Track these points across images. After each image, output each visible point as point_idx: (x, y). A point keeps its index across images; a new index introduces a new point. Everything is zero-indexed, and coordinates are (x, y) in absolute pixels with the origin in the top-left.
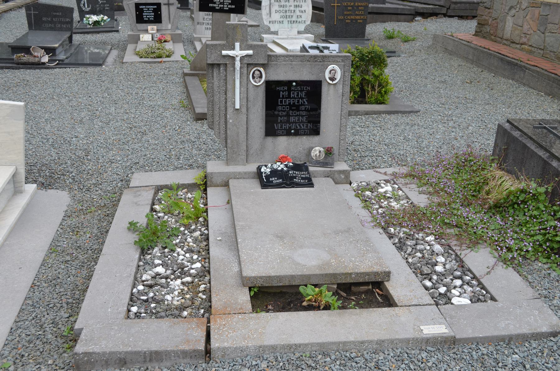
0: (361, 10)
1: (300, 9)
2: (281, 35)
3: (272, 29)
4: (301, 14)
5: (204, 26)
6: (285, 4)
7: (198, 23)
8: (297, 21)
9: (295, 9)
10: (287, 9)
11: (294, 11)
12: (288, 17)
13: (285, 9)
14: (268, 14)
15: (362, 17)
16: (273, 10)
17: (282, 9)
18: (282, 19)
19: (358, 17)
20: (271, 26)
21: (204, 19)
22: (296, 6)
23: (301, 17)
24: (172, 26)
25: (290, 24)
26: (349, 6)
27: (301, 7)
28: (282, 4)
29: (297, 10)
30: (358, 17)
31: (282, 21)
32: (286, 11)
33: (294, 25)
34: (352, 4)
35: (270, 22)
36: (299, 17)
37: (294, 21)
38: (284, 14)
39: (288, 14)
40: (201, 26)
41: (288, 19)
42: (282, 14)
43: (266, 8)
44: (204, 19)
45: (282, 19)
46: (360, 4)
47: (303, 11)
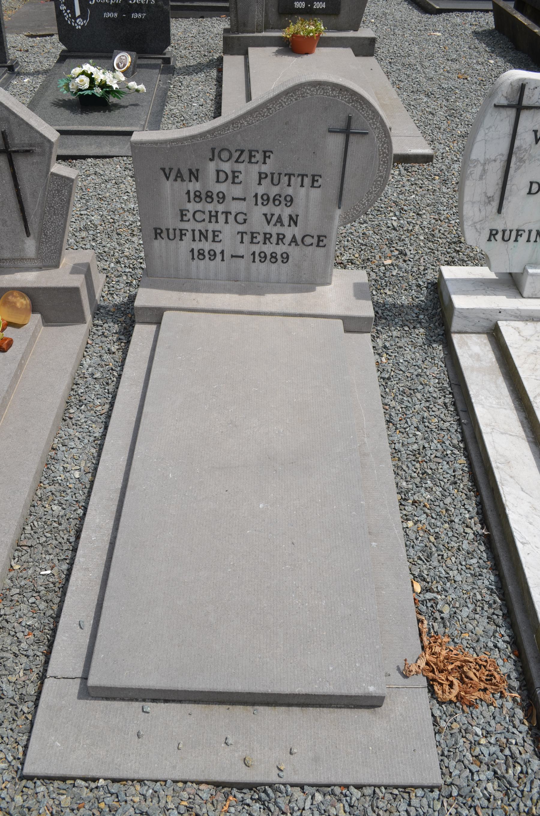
5: (186, 244)
14: (490, 200)
21: (182, 214)
24: (40, 243)
35: (493, 234)
40: (172, 244)
43: (484, 171)
44: (182, 214)
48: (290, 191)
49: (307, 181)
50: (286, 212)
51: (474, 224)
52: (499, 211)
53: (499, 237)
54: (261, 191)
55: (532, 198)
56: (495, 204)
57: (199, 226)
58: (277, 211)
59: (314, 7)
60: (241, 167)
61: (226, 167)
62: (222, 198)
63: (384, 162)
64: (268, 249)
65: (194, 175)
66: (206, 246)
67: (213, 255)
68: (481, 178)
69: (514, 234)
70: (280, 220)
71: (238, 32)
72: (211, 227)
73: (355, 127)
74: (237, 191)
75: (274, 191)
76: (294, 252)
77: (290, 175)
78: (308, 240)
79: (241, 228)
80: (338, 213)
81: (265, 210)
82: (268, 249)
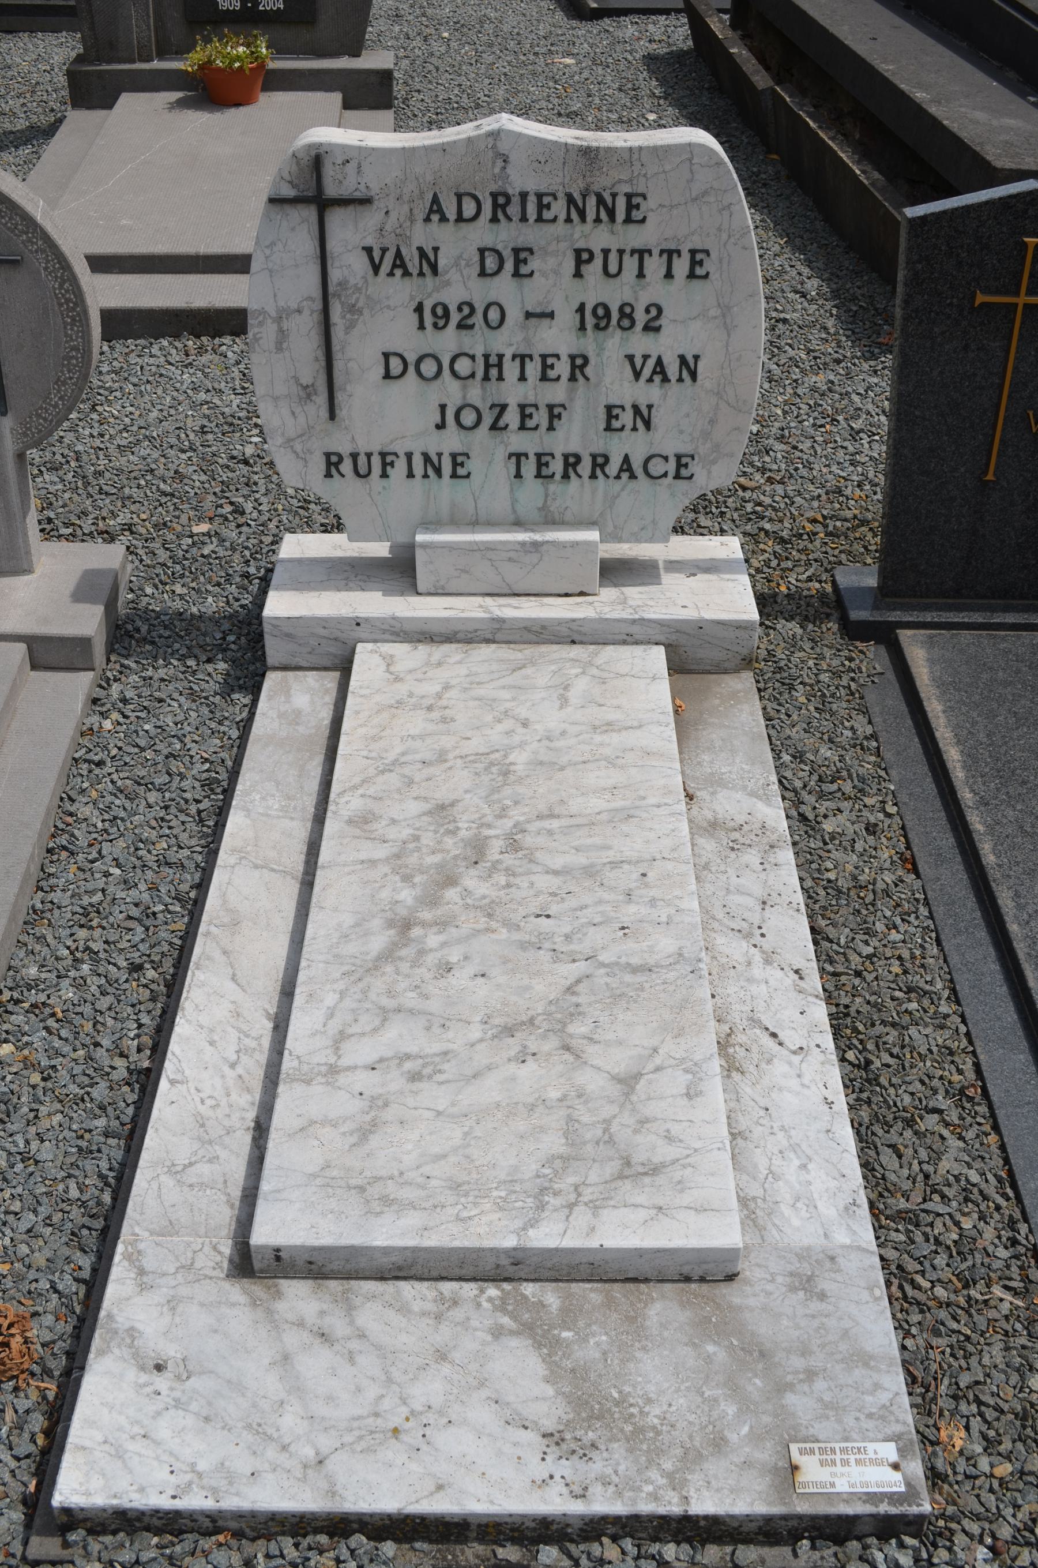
1: (640, 343)
6: (480, 292)
8: (600, 462)
9: (589, 344)
11: (579, 365)
12: (511, 417)
13: (478, 342)
14: (308, 392)
18: (451, 441)
23: (643, 417)
28: (452, 297)
31: (457, 460)
35: (332, 464)
36: (627, 418)
37: (571, 462)
38: (475, 393)
41: (518, 441)
42: (451, 391)
43: (282, 335)
45: (451, 441)
47: (673, 369)
51: (289, 442)
52: (332, 416)
53: (346, 467)
55: (395, 386)
56: (322, 399)
59: (261, 8)
63: (73, 319)
68: (279, 347)
69: (376, 461)
71: (100, 60)
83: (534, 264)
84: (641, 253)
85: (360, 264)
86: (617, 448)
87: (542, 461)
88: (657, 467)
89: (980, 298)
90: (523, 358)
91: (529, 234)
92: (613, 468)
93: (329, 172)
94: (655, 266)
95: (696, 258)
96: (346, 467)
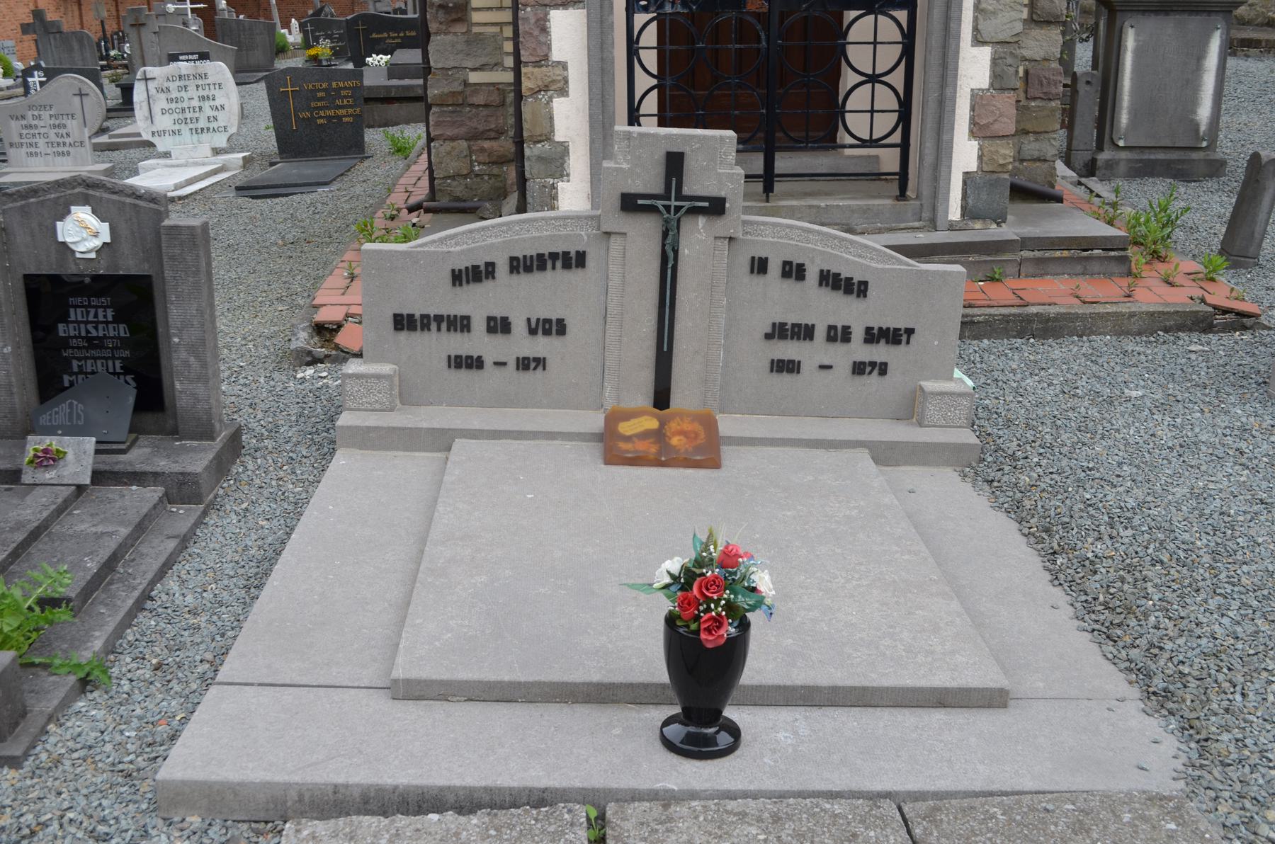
0: (345, 97)
1: (212, 103)
2: (177, 159)
3: (161, 147)
4: (215, 113)
5: (24, 150)
7: (11, 145)
8: (208, 129)
9: (202, 104)
10: (185, 105)
11: (200, 108)
12: (189, 121)
13: (180, 105)
14: (147, 118)
15: (351, 111)
16: (156, 109)
17: (173, 106)
19: (341, 112)
20: (155, 140)
21: (21, 135)
22: (203, 98)
23: (215, 119)
25: (195, 136)
26: (319, 90)
27: (213, 99)
28: (173, 96)
29: (206, 105)
30: (341, 112)
31: (179, 131)
32: (183, 110)
33: (205, 136)
34: (325, 85)
35: (153, 133)
36: (212, 119)
37: (202, 129)
38: (181, 116)
39: (188, 115)
40: (18, 150)
41: (191, 126)
42: (176, 116)
43: (141, 106)
44: (21, 135)
45: (177, 127)
46: (341, 84)
47: (219, 108)
48: (64, 122)
49: (70, 117)
50: (64, 131)
53: (156, 134)
54: (52, 122)
57: (29, 141)
58: (60, 131)
60: (41, 113)
61: (36, 113)
62: (36, 127)
64: (60, 149)
65: (23, 117)
66: (33, 150)
67: (36, 154)
68: (140, 109)
70: (62, 136)
72: (34, 140)
73: (78, 92)
74: (42, 123)
75: (57, 122)
76: (71, 149)
77: (62, 115)
78: (77, 144)
79: (47, 140)
80: (86, 130)
81: (55, 131)
82: (60, 149)
83: (188, 88)
84: (209, 85)
85: (155, 91)
86: (212, 125)
87: (196, 130)
88: (220, 129)
89: (281, 90)
90: (189, 108)
91: (187, 83)
92: (211, 130)
93: (147, 74)
94: (212, 87)
95: (220, 85)
96: (156, 134)
